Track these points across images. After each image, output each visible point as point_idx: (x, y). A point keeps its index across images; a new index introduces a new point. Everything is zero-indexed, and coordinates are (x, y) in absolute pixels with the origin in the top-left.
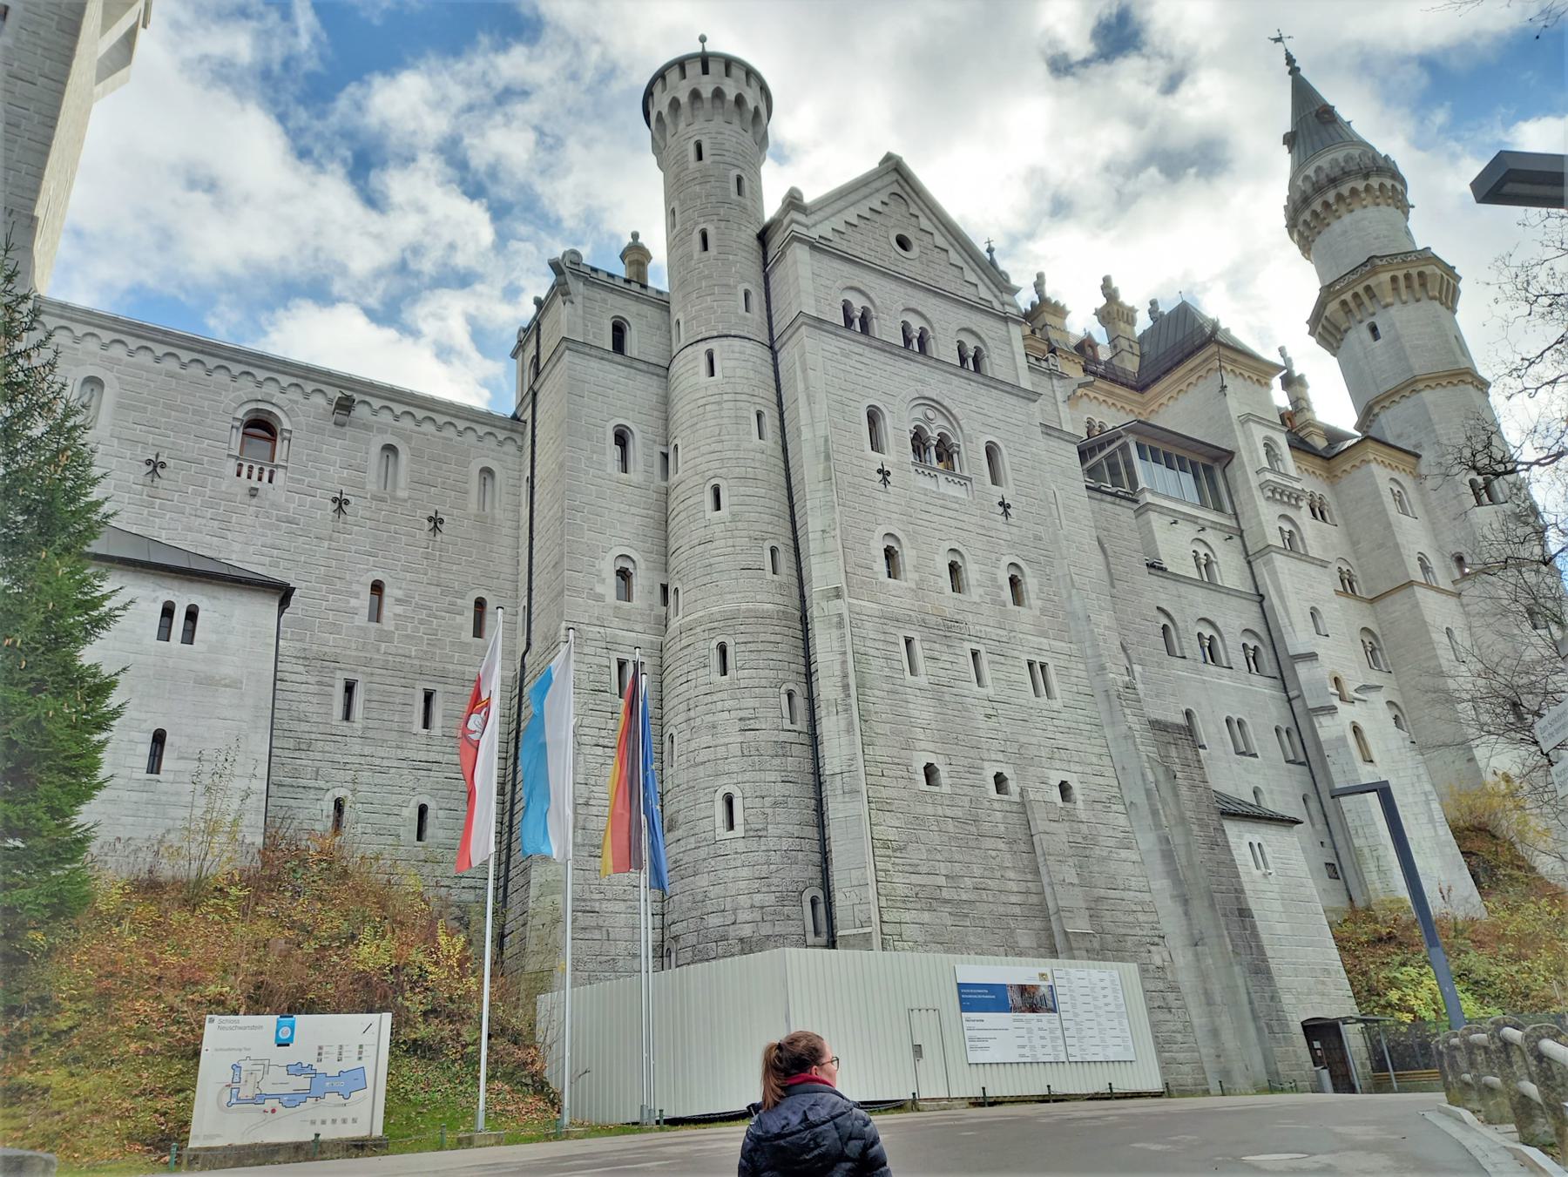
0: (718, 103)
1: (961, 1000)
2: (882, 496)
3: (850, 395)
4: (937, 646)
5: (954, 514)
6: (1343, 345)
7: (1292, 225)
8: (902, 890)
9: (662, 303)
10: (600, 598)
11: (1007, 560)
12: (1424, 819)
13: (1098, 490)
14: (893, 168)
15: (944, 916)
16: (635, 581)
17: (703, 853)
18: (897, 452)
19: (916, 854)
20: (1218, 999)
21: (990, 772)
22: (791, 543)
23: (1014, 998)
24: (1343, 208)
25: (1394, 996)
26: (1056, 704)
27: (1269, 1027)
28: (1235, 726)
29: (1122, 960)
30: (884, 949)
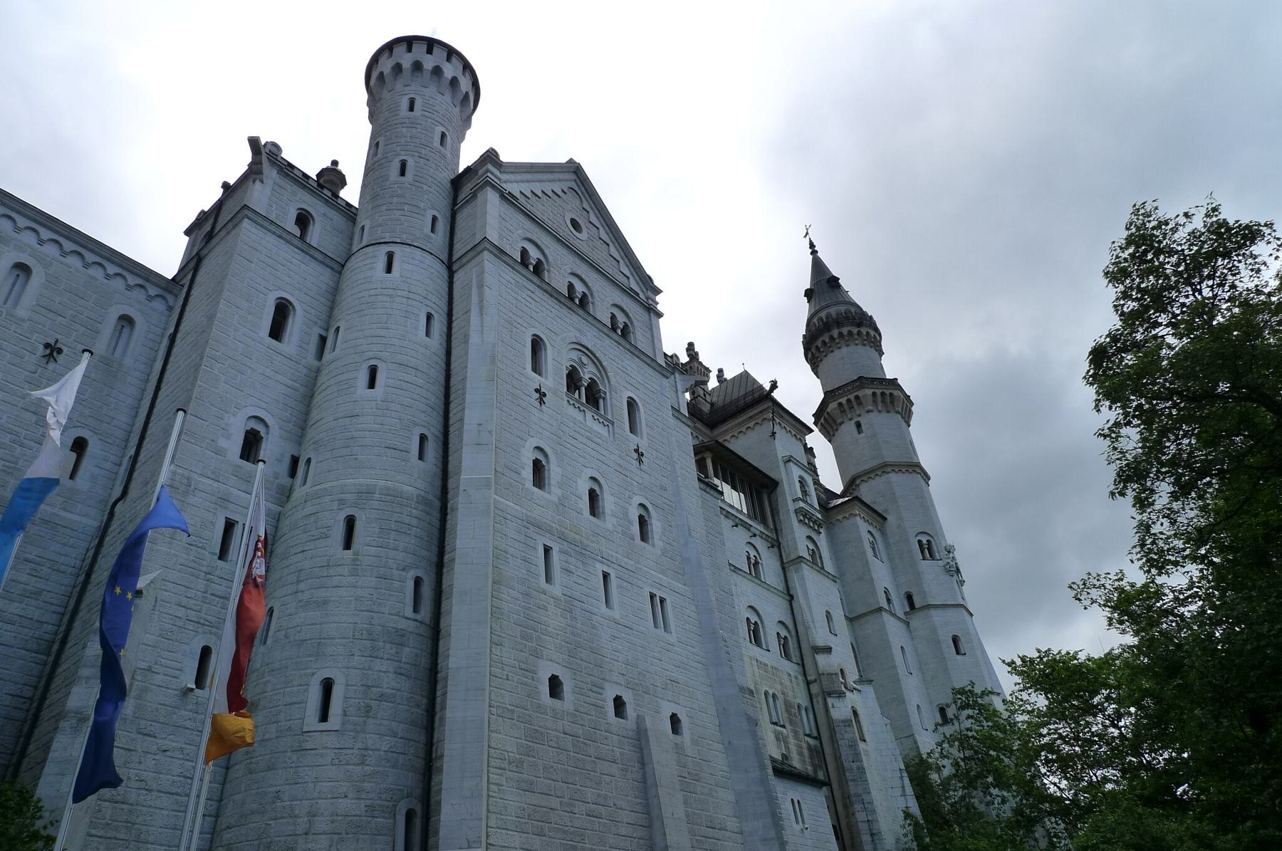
0: (435, 78)
2: (536, 412)
5: (598, 448)
10: (219, 452)
11: (638, 499)
12: (899, 792)
18: (554, 381)
21: (610, 693)
24: (842, 342)
26: (672, 638)
28: (771, 700)
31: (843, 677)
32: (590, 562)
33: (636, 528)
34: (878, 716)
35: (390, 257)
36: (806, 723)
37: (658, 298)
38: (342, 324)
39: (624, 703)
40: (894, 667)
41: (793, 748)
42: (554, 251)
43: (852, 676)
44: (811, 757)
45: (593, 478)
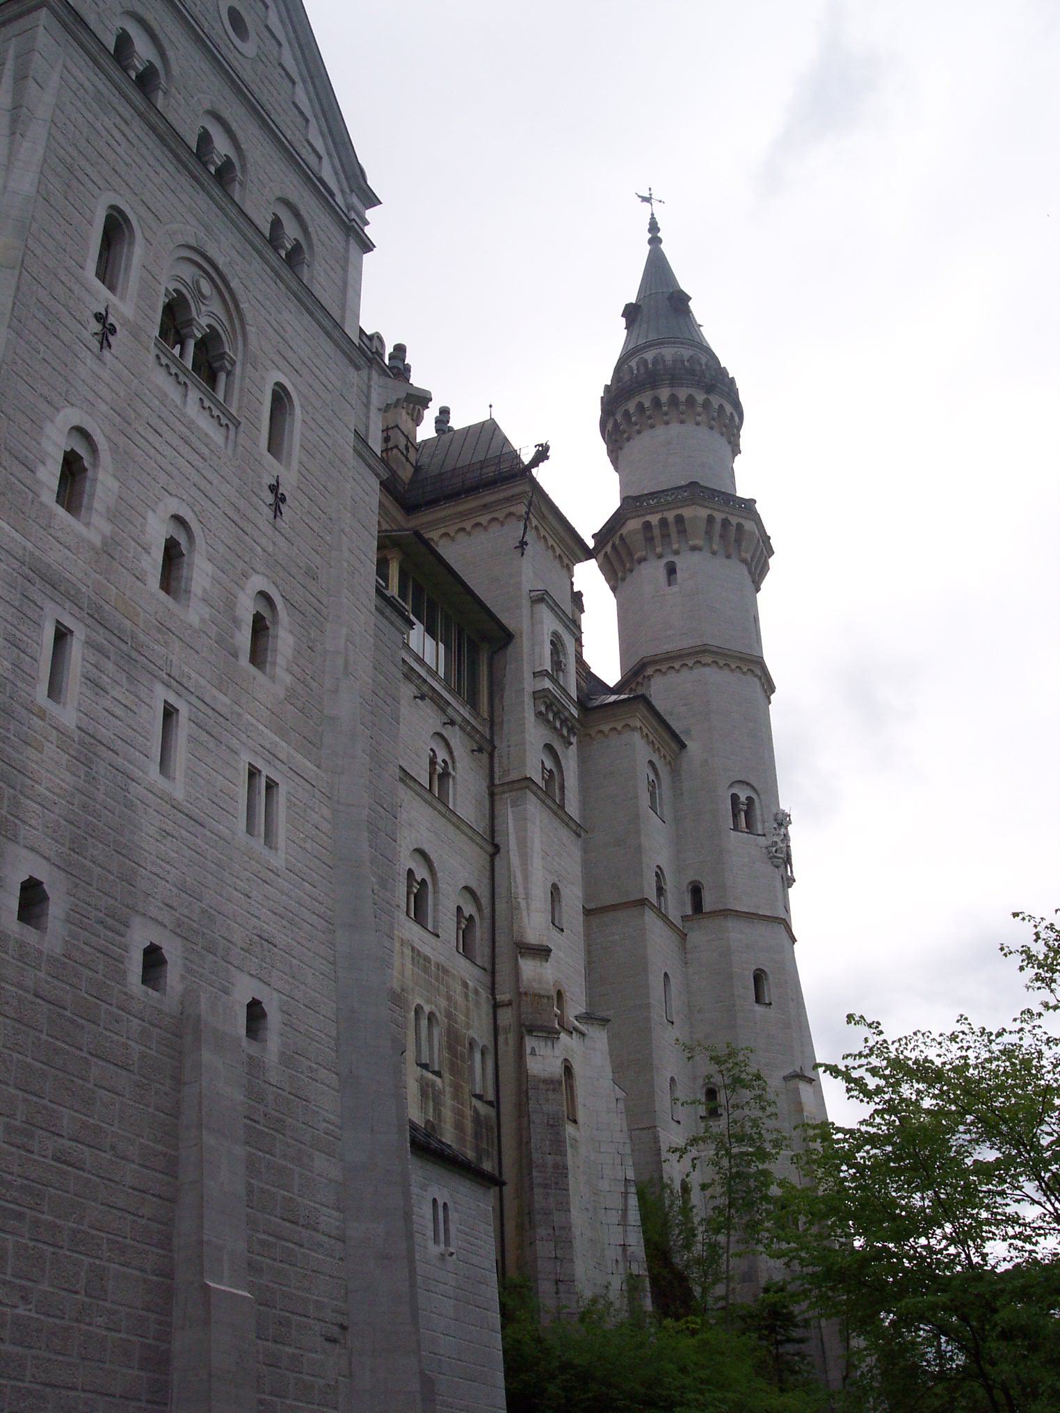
3: (89, 170)
4: (110, 666)
5: (199, 463)
11: (258, 582)
12: (614, 1217)
18: (137, 307)
21: (141, 936)
26: (278, 860)
31: (560, 1007)
33: (244, 638)
34: (606, 1082)
36: (479, 1073)
37: (370, 214)
39: (163, 962)
40: (648, 1006)
41: (448, 1114)
42: (184, 59)
43: (575, 1006)
44: (477, 1135)
45: (179, 520)
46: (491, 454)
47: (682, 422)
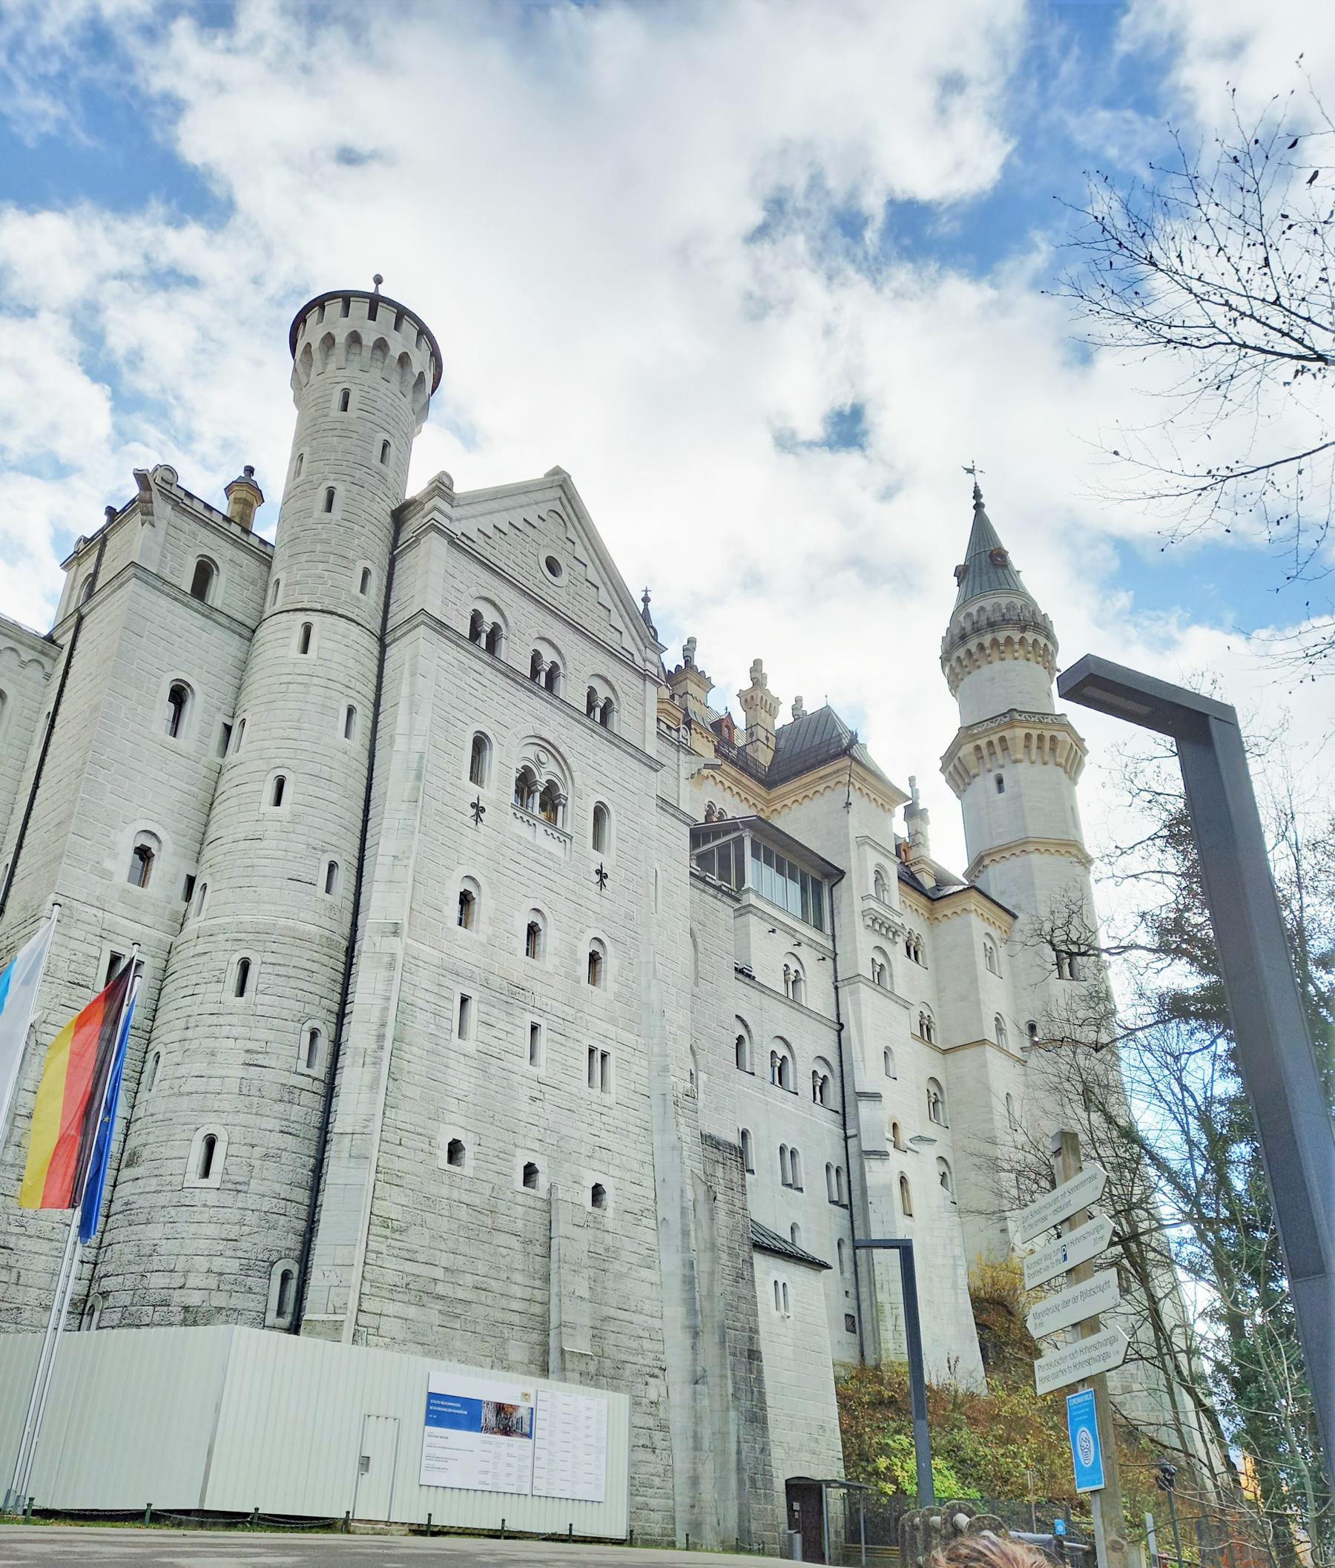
1: (428, 1412)
4: (495, 1012)
6: (970, 788)
7: (945, 659)
8: (391, 1277)
9: (264, 555)
10: (106, 875)
13: (703, 880)
14: (560, 482)
15: (433, 1313)
16: (156, 865)
17: (162, 1199)
18: (499, 788)
19: (415, 1239)
20: (706, 1446)
22: (355, 862)
23: (489, 1416)
24: (995, 655)
25: (882, 1463)
27: (753, 1481)
29: (617, 1389)
30: (354, 1342)
32: (517, 1012)
35: (307, 629)
38: (247, 716)
46: (826, 737)
47: (1003, 659)
